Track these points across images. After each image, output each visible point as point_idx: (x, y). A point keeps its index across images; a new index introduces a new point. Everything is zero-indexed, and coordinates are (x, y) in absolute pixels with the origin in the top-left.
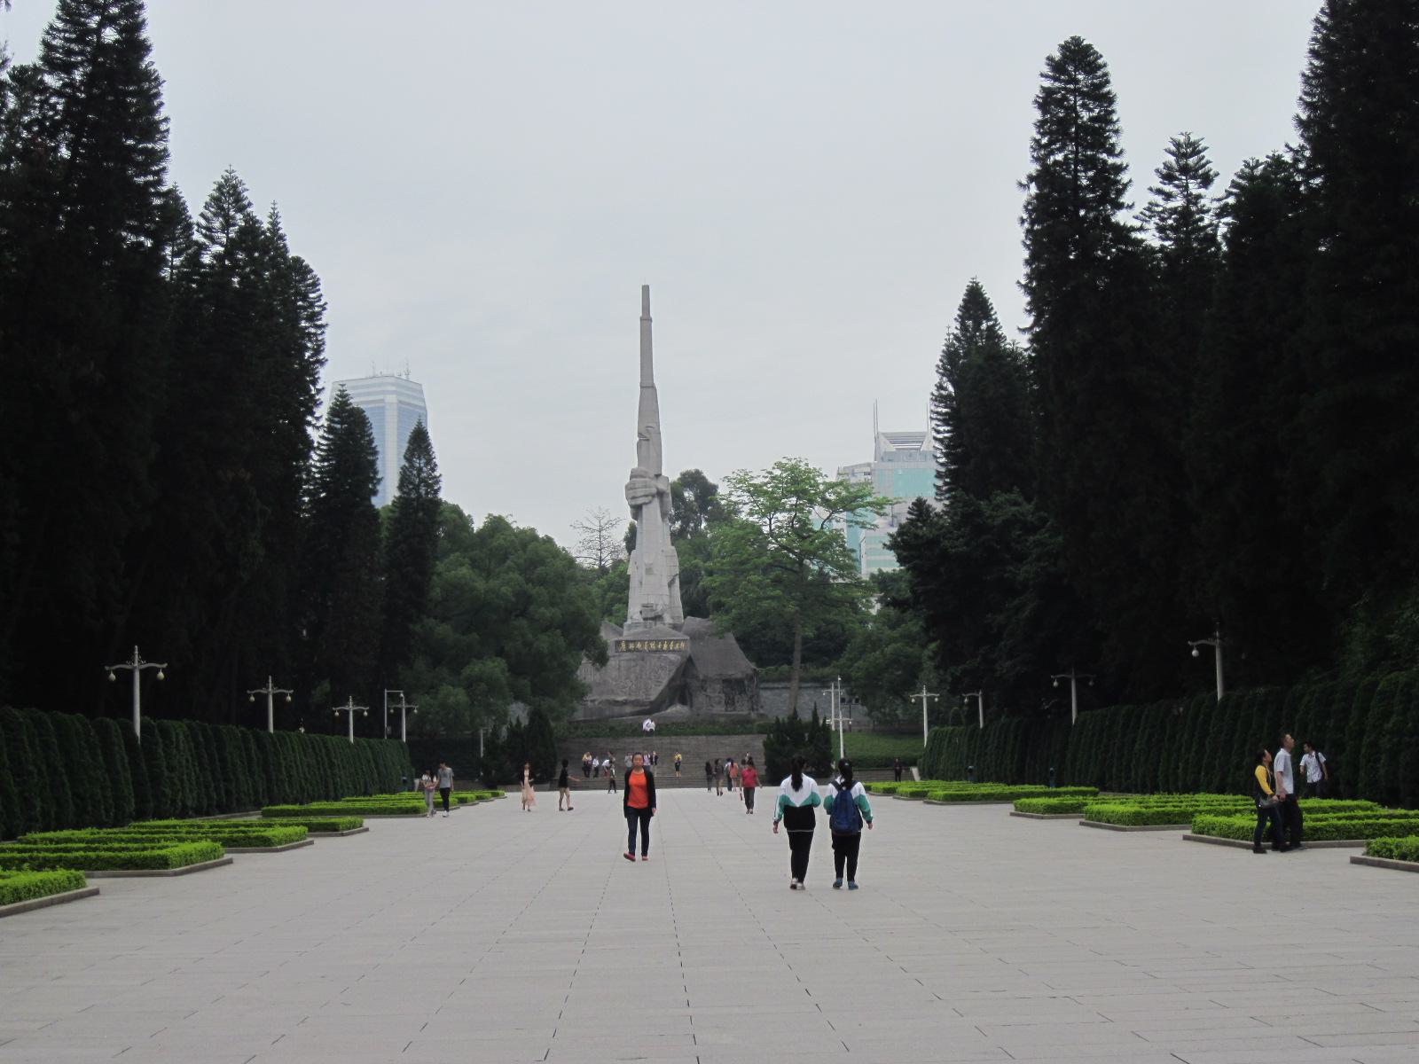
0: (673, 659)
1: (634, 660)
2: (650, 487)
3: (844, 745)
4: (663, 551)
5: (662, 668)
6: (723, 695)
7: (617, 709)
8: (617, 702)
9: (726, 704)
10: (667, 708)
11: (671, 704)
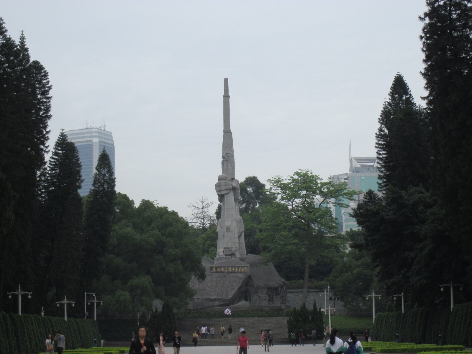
0: (241, 276)
2: (228, 185)
3: (331, 323)
4: (235, 219)
6: (267, 296)
7: (211, 303)
8: (211, 299)
9: (269, 300)
10: (237, 303)
11: (239, 301)
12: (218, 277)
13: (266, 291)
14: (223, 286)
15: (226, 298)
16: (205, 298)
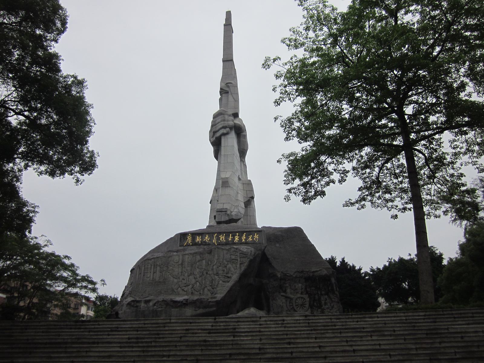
0: (245, 250)
1: (201, 254)
2: (228, 121)
4: (239, 179)
5: (232, 261)
6: (306, 296)
9: (311, 306)
10: (238, 312)
12: (196, 253)
13: (303, 287)
14: (207, 273)
15: (212, 298)
16: (163, 301)
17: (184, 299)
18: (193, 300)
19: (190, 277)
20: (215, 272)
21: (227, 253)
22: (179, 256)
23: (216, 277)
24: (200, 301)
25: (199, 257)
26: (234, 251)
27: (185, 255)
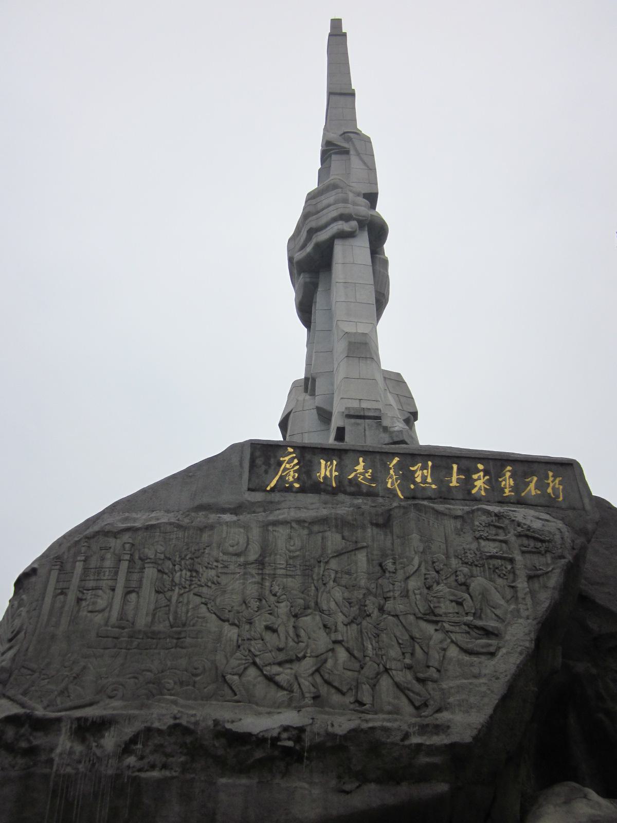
0: (537, 525)
1: (342, 524)
8: (244, 738)
12: (323, 521)
15: (424, 729)
16: (177, 728)
17: (286, 729)
18: (333, 736)
19: (306, 621)
20: (422, 608)
21: (459, 532)
22: (247, 528)
23: (430, 629)
24: (368, 743)
25: (338, 537)
26: (489, 525)
27: (275, 523)
